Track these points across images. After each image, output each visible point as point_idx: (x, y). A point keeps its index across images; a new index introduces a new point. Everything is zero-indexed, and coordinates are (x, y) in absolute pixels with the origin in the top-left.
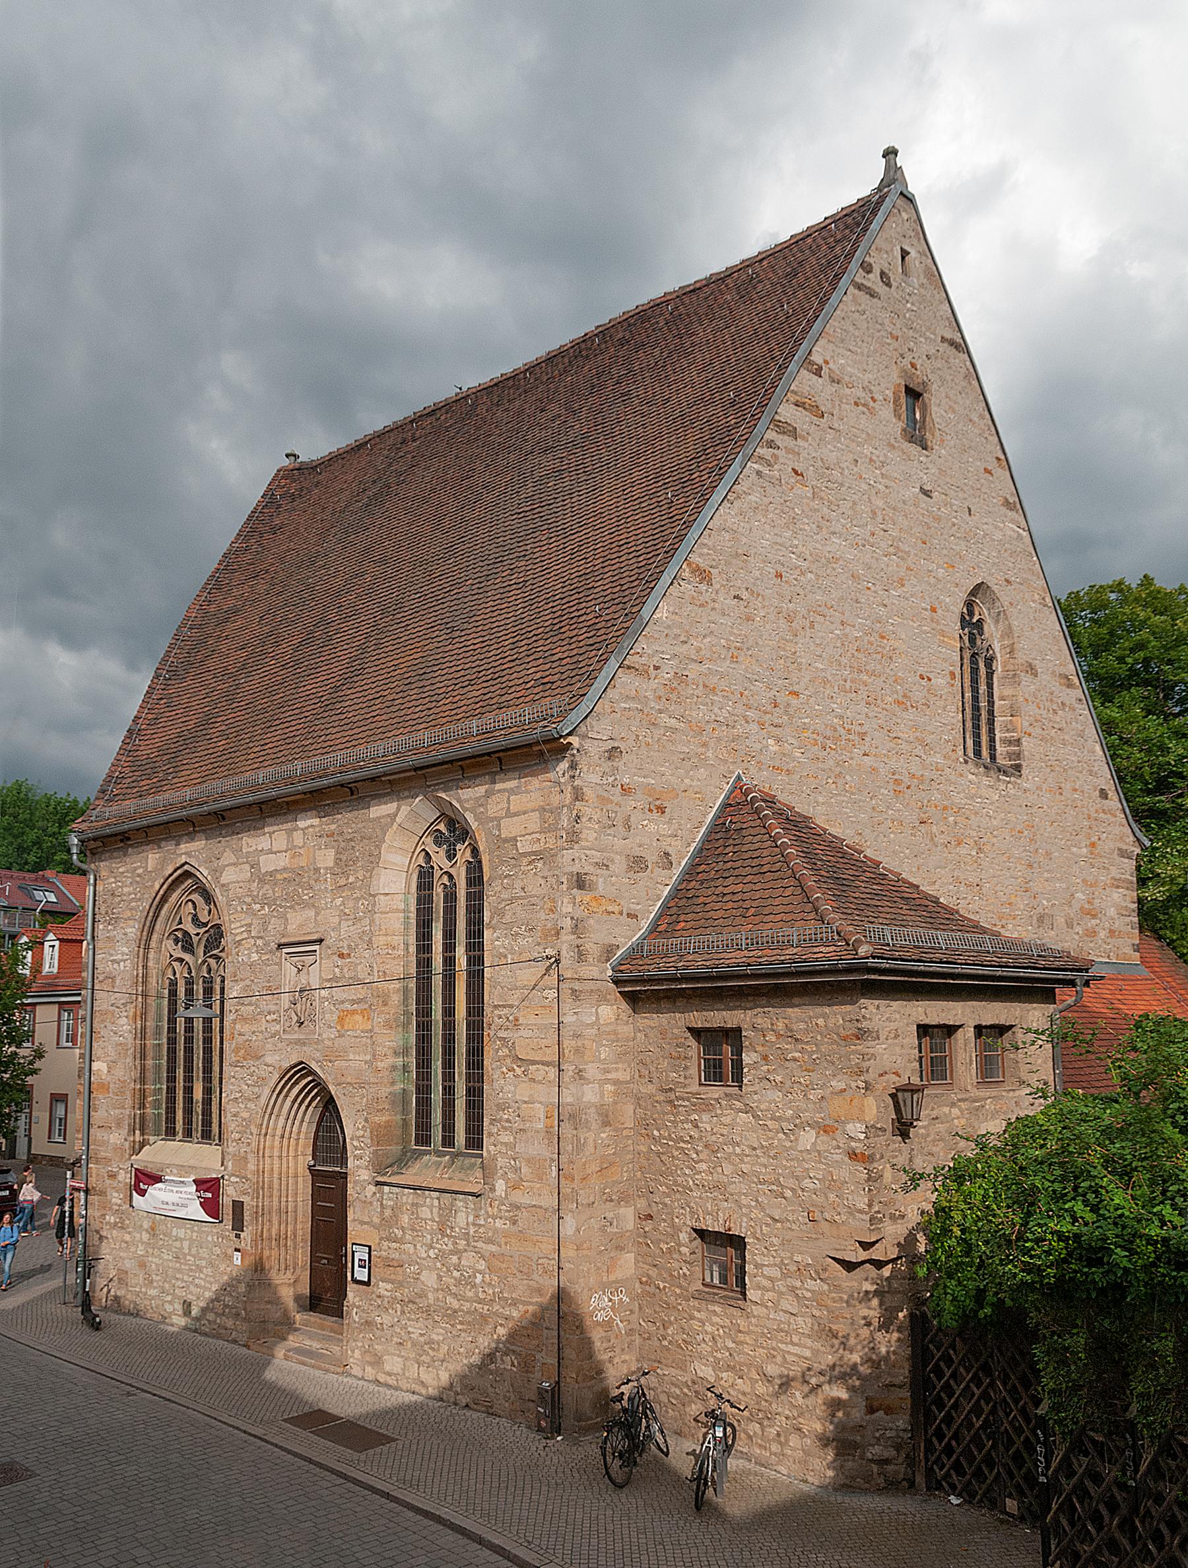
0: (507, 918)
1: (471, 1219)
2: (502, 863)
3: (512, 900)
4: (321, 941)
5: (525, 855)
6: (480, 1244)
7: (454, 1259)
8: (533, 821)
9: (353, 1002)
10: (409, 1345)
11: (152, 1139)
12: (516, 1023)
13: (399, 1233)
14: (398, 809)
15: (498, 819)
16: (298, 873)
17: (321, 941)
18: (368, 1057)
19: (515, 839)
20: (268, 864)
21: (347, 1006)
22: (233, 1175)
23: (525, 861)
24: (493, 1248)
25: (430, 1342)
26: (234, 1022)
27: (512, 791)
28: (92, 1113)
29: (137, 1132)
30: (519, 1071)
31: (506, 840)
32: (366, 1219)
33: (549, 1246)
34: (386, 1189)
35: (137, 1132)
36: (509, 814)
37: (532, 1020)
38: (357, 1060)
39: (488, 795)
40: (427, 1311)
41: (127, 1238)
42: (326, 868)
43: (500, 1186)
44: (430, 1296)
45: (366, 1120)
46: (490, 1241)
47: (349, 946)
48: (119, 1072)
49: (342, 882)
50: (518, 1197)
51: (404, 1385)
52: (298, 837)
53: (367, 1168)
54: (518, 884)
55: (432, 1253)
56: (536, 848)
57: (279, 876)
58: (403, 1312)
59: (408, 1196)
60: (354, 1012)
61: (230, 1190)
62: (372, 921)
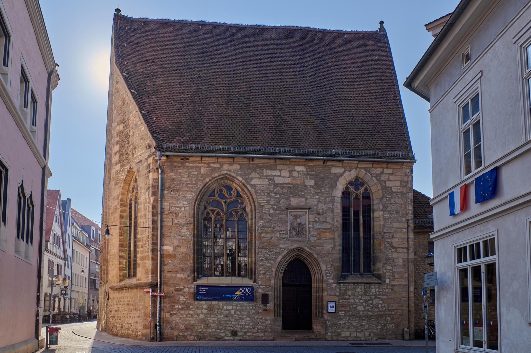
0: (389, 209)
1: (377, 290)
2: (386, 193)
3: (390, 204)
4: (310, 209)
5: (395, 192)
6: (380, 297)
7: (370, 302)
8: (398, 184)
9: (325, 229)
10: (352, 327)
11: (200, 276)
12: (393, 237)
13: (348, 297)
14: (345, 172)
15: (385, 181)
16: (295, 186)
17: (310, 209)
18: (332, 246)
19: (391, 188)
20: (277, 180)
21: (321, 230)
22: (261, 285)
23: (395, 194)
24: (385, 297)
25: (361, 325)
26: (261, 233)
27: (390, 174)
28: (163, 267)
29: (196, 273)
30: (393, 250)
31: (388, 187)
32: (333, 294)
33: (405, 294)
34: (342, 285)
35: (196, 273)
36: (389, 180)
37: (398, 236)
38: (327, 247)
39: (382, 173)
40: (360, 317)
41: (192, 312)
42: (311, 186)
43: (387, 281)
44: (361, 313)
45: (332, 265)
46: (383, 295)
47: (322, 212)
48: (183, 249)
49: (319, 191)
50: (393, 283)
51: (351, 339)
52: (295, 174)
53: (332, 279)
54: (393, 200)
55: (361, 301)
56: (399, 191)
57: (285, 185)
58: (349, 319)
59: (351, 286)
60: (325, 232)
61: (260, 291)
62: (333, 205)
